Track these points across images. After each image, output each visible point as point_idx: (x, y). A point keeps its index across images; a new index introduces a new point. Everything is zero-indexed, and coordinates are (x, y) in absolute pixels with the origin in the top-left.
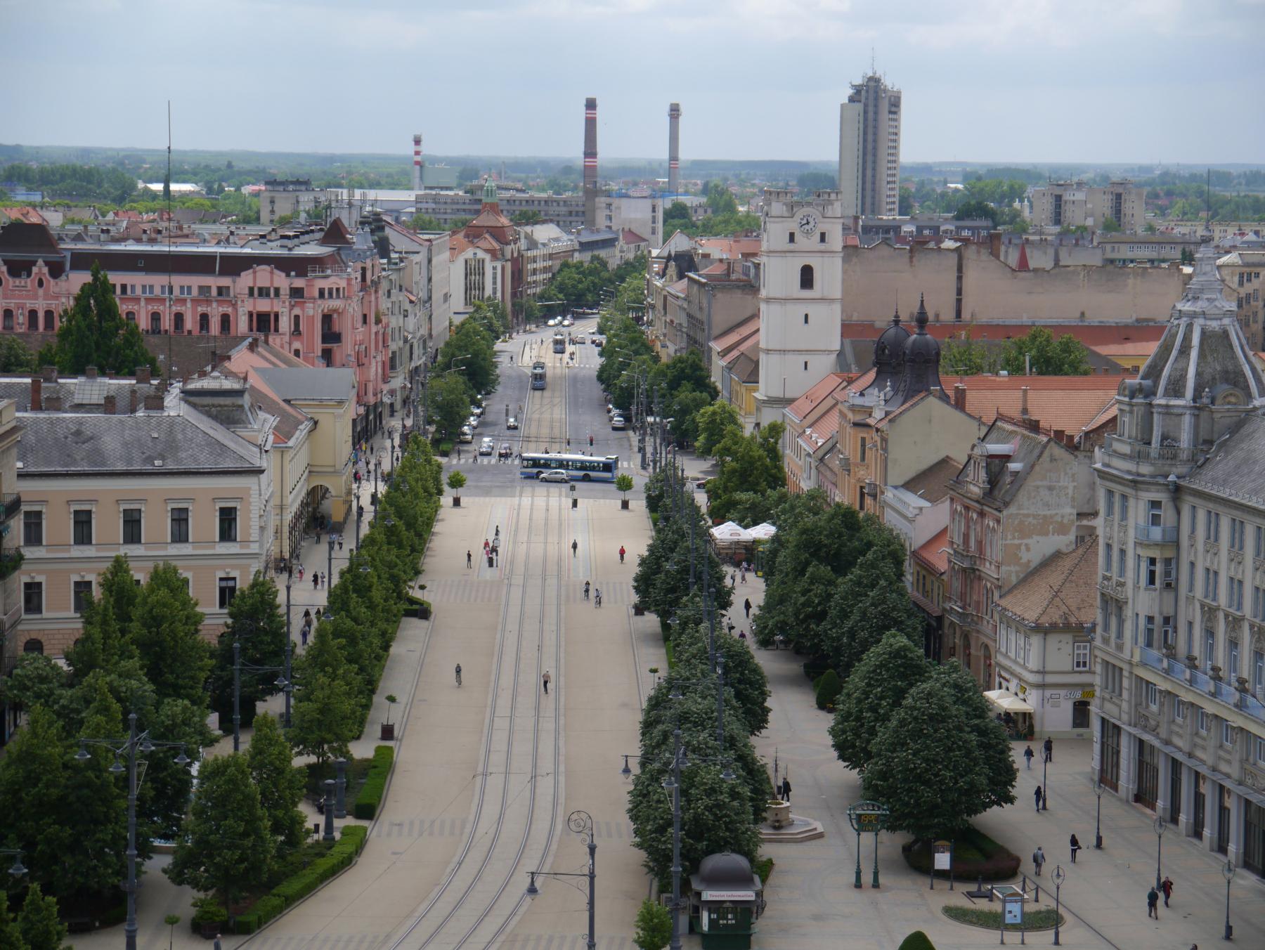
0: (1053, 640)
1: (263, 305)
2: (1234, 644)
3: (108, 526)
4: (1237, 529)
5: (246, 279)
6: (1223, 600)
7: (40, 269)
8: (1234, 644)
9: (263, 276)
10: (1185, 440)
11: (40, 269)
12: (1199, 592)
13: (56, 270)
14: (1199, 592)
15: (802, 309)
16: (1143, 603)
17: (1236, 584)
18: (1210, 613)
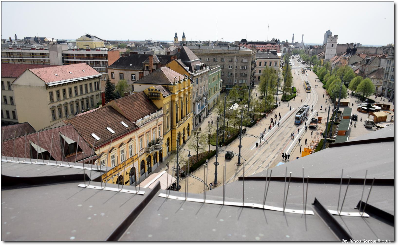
0: (375, 80)
1: (269, 48)
3: (263, 64)
5: (267, 45)
7: (245, 44)
9: (269, 45)
11: (245, 44)
13: (247, 44)
15: (331, 49)
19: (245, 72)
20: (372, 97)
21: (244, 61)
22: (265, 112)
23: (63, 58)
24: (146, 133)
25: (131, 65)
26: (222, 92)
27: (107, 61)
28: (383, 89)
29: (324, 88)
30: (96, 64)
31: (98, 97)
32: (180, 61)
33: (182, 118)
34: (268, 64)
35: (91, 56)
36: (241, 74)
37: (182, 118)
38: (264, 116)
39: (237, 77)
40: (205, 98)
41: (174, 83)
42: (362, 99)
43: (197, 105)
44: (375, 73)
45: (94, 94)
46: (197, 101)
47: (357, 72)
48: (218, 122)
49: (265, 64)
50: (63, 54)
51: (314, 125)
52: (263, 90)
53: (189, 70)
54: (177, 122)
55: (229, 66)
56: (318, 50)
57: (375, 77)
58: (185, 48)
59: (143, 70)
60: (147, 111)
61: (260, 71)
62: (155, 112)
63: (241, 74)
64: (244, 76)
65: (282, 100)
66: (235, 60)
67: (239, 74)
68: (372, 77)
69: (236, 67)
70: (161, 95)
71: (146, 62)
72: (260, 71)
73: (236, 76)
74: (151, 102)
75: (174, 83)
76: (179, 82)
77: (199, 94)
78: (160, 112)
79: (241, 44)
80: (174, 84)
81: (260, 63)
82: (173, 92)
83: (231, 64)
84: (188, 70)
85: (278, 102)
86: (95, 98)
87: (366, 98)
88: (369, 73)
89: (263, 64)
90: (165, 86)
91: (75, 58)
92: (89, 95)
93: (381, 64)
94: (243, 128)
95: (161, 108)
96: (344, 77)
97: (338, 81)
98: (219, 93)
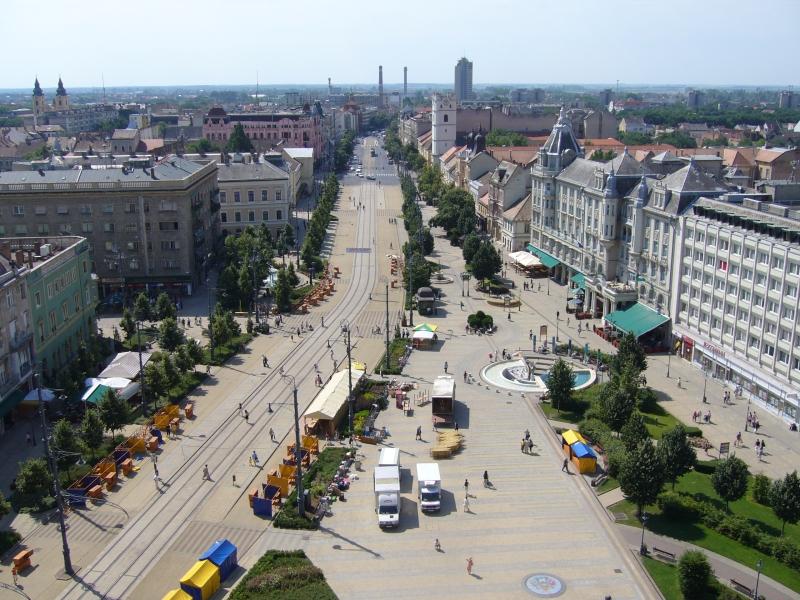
1: (286, 130)
2: (570, 225)
5: (281, 123)
7: (222, 122)
8: (570, 225)
9: (286, 121)
13: (226, 122)
17: (571, 207)
21: (167, 207)
39: (153, 253)
69: (148, 225)
79: (210, 122)
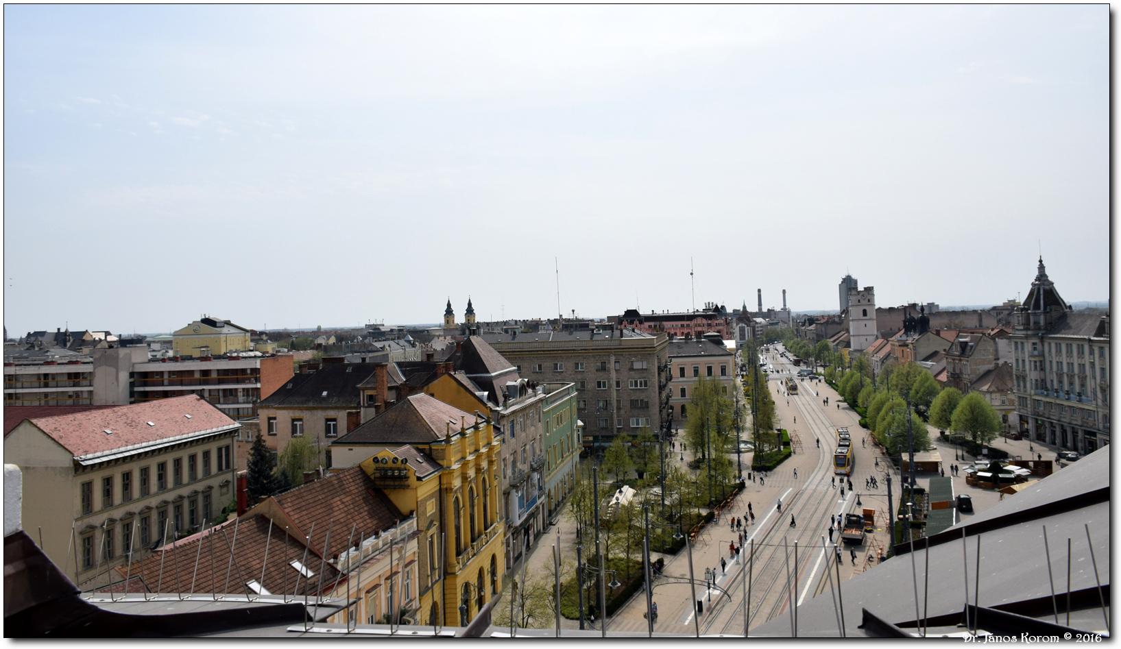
0: (994, 395)
1: (700, 329)
2: (1071, 384)
3: (689, 372)
4: (1069, 347)
6: (1065, 370)
8: (1071, 384)
9: (699, 321)
10: (1042, 322)
12: (1055, 369)
13: (641, 322)
14: (1055, 369)
16: (1032, 375)
17: (1070, 365)
18: (1060, 376)
19: (642, 396)
20: (998, 443)
21: (637, 365)
22: (709, 505)
23: (132, 385)
24: (368, 592)
25: (325, 393)
26: (583, 456)
27: (259, 385)
28: (1022, 419)
29: (864, 426)
30: (225, 396)
31: (224, 490)
32: (461, 376)
33: (473, 540)
34: (703, 371)
35: (214, 375)
36: (634, 404)
37: (473, 540)
38: (710, 519)
39: (622, 412)
40: (536, 476)
41: (448, 437)
42: (974, 450)
43: (515, 497)
44: (992, 377)
45: (215, 482)
46: (514, 486)
47: (943, 377)
48: (580, 543)
49: (696, 372)
50: (132, 375)
51: (855, 533)
52: (699, 442)
53: (489, 398)
54: (458, 553)
55: (599, 383)
56: (830, 326)
57: (993, 388)
58: (474, 339)
59: (358, 406)
60: (372, 524)
61: (683, 391)
62: (393, 525)
63: (634, 404)
64: (640, 406)
65: (754, 468)
66: (612, 365)
67: (626, 404)
68: (985, 388)
69: (618, 384)
70: (410, 474)
71: (368, 383)
72: (683, 391)
73: (619, 409)
74: (382, 496)
75: (448, 437)
76: (462, 434)
77: (519, 466)
78: (411, 525)
79: (625, 323)
80: (448, 440)
81: (682, 370)
82: (444, 463)
83: (601, 377)
84: (485, 400)
85: (745, 474)
86: (215, 494)
87: (981, 447)
88: (974, 377)
89: (689, 372)
90: (421, 447)
91: (166, 382)
92: (200, 487)
93: (1001, 353)
94: (654, 557)
95: (412, 512)
96: (912, 392)
97: (899, 405)
98: (577, 458)
